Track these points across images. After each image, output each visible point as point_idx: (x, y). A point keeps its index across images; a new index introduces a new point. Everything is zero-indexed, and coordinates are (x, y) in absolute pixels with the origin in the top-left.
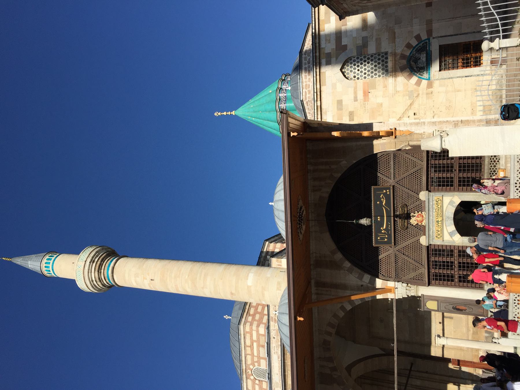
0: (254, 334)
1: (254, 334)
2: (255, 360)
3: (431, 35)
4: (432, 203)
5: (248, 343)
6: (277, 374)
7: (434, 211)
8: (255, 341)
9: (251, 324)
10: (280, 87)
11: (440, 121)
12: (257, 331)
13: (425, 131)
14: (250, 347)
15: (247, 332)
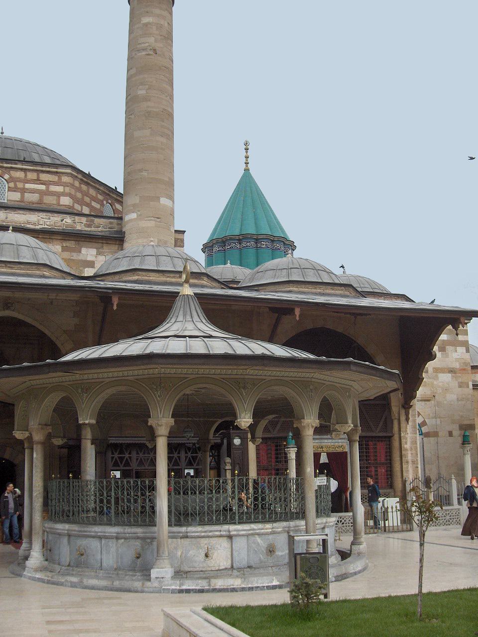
0: (60, 189)
1: (60, 189)
2: (17, 183)
3: (425, 437)
4: (340, 442)
5: (44, 177)
6: (6, 218)
7: (332, 444)
8: (48, 188)
9: (72, 185)
10: (287, 243)
11: (417, 448)
12: (64, 194)
13: (409, 435)
14: (38, 179)
15: (60, 179)
